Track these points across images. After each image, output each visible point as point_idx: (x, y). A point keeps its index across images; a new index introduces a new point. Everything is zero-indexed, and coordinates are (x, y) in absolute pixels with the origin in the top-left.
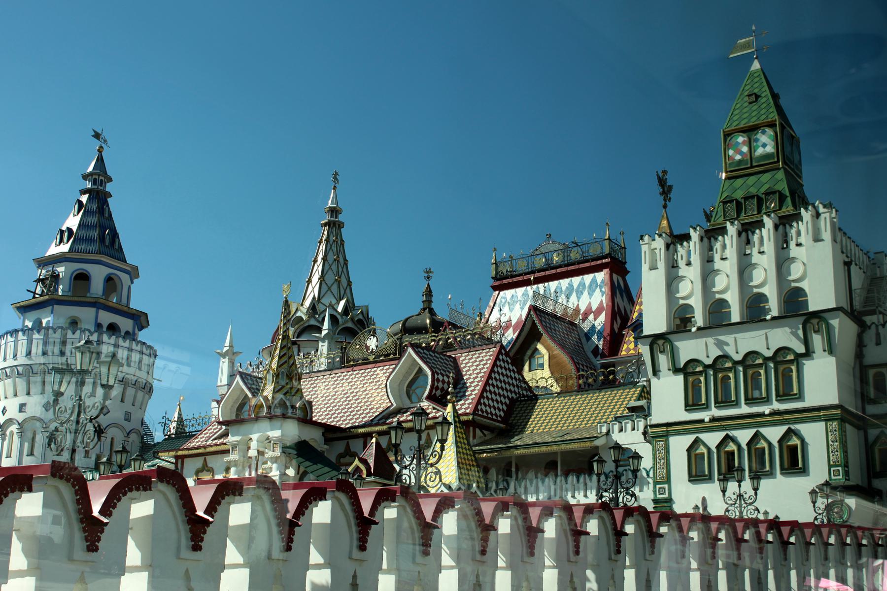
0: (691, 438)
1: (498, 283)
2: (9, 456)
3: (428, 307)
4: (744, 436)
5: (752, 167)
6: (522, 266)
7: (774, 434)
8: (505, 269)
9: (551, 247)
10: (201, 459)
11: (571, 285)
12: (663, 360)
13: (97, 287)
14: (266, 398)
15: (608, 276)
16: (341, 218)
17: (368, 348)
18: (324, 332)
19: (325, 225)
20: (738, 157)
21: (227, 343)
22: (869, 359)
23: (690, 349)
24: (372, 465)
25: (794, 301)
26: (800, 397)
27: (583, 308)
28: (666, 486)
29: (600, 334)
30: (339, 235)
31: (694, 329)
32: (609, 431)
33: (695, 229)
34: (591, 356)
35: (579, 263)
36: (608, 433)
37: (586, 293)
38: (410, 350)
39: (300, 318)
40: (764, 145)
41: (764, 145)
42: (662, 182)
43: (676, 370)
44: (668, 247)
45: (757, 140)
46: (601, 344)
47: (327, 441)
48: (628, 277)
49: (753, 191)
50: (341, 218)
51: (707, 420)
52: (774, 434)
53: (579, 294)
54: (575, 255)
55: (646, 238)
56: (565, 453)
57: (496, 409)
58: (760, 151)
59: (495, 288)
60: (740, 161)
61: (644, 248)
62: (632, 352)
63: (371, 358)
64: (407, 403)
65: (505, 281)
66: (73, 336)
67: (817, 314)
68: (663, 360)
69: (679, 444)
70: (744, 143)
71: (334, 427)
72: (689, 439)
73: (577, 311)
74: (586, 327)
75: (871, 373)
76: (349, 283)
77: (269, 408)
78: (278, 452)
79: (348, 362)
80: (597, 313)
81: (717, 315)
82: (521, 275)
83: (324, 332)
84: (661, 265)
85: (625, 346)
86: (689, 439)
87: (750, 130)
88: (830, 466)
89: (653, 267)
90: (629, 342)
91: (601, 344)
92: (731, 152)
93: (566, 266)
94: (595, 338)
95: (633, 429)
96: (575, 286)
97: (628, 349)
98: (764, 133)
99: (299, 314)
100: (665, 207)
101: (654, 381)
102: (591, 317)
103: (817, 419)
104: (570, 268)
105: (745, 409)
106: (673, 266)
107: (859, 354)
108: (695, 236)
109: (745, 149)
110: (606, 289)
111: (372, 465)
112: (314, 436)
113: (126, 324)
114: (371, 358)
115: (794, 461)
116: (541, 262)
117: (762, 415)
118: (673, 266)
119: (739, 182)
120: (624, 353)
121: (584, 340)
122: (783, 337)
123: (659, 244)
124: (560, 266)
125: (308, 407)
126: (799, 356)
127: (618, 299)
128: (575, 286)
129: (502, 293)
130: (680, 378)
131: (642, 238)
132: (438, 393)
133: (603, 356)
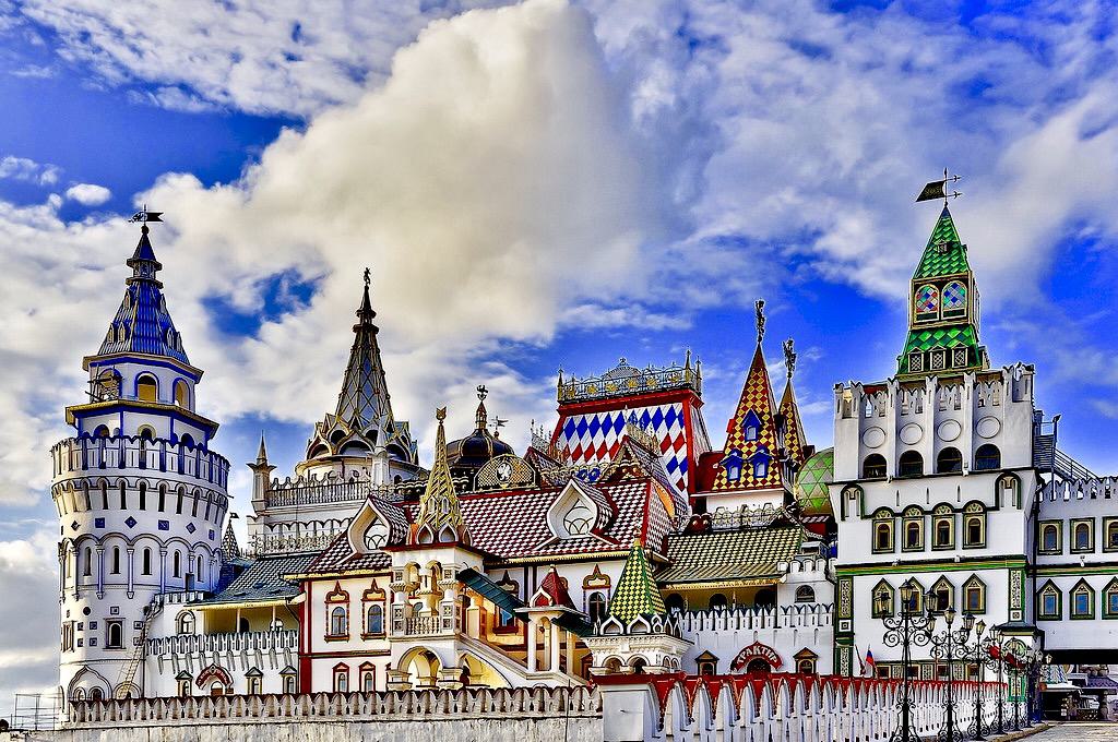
0: (876, 579)
2: (88, 573)
3: (481, 431)
10: (334, 582)
16: (374, 322)
17: (499, 476)
27: (661, 438)
28: (1012, 619)
36: (788, 571)
47: (486, 570)
62: (724, 487)
66: (153, 448)
67: (1008, 472)
69: (864, 586)
72: (874, 580)
78: (452, 579)
79: (477, 488)
85: (717, 482)
86: (874, 580)
90: (721, 478)
95: (814, 568)
97: (720, 485)
112: (476, 563)
113: (197, 436)
120: (715, 488)
122: (982, 488)
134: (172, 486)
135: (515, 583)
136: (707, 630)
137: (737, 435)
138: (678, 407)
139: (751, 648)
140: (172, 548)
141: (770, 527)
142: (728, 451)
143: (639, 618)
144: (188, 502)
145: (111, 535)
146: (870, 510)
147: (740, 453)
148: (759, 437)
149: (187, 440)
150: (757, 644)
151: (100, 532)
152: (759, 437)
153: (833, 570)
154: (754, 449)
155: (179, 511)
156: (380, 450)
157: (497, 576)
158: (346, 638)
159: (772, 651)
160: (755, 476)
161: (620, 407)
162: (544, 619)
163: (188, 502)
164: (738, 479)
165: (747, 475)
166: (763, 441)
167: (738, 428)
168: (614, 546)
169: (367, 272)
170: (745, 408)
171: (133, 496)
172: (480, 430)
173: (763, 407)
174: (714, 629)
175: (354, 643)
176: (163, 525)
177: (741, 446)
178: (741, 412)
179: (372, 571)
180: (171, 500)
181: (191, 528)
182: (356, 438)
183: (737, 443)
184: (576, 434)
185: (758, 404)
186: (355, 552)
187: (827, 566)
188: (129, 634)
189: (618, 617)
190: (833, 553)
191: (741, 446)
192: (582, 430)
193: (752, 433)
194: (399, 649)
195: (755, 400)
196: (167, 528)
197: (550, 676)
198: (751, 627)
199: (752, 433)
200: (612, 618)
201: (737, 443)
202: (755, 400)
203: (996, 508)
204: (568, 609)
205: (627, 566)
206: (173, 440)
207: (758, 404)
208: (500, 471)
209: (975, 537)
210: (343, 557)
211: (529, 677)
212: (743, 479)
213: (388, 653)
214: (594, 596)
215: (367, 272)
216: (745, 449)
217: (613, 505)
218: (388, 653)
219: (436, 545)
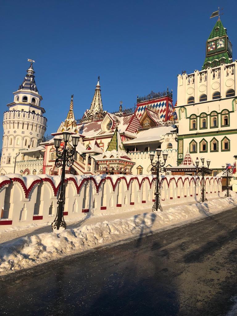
13: (29, 101)
20: (212, 49)
40: (221, 45)
41: (221, 45)
43: (187, 118)
48: (172, 102)
58: (219, 47)
68: (183, 115)
70: (214, 45)
80: (164, 112)
92: (209, 48)
98: (221, 40)
129: (139, 107)
134: (16, 122)
138: (165, 102)
140: (10, 138)
144: (30, 127)
145: (11, 135)
146: (188, 116)
149: (34, 112)
151: (15, 135)
155: (27, 129)
163: (30, 127)
169: (99, 77)
171: (16, 125)
176: (23, 132)
180: (25, 126)
181: (31, 134)
188: (12, 160)
190: (178, 132)
196: (24, 134)
205: (112, 139)
206: (30, 112)
209: (227, 123)
215: (99, 77)
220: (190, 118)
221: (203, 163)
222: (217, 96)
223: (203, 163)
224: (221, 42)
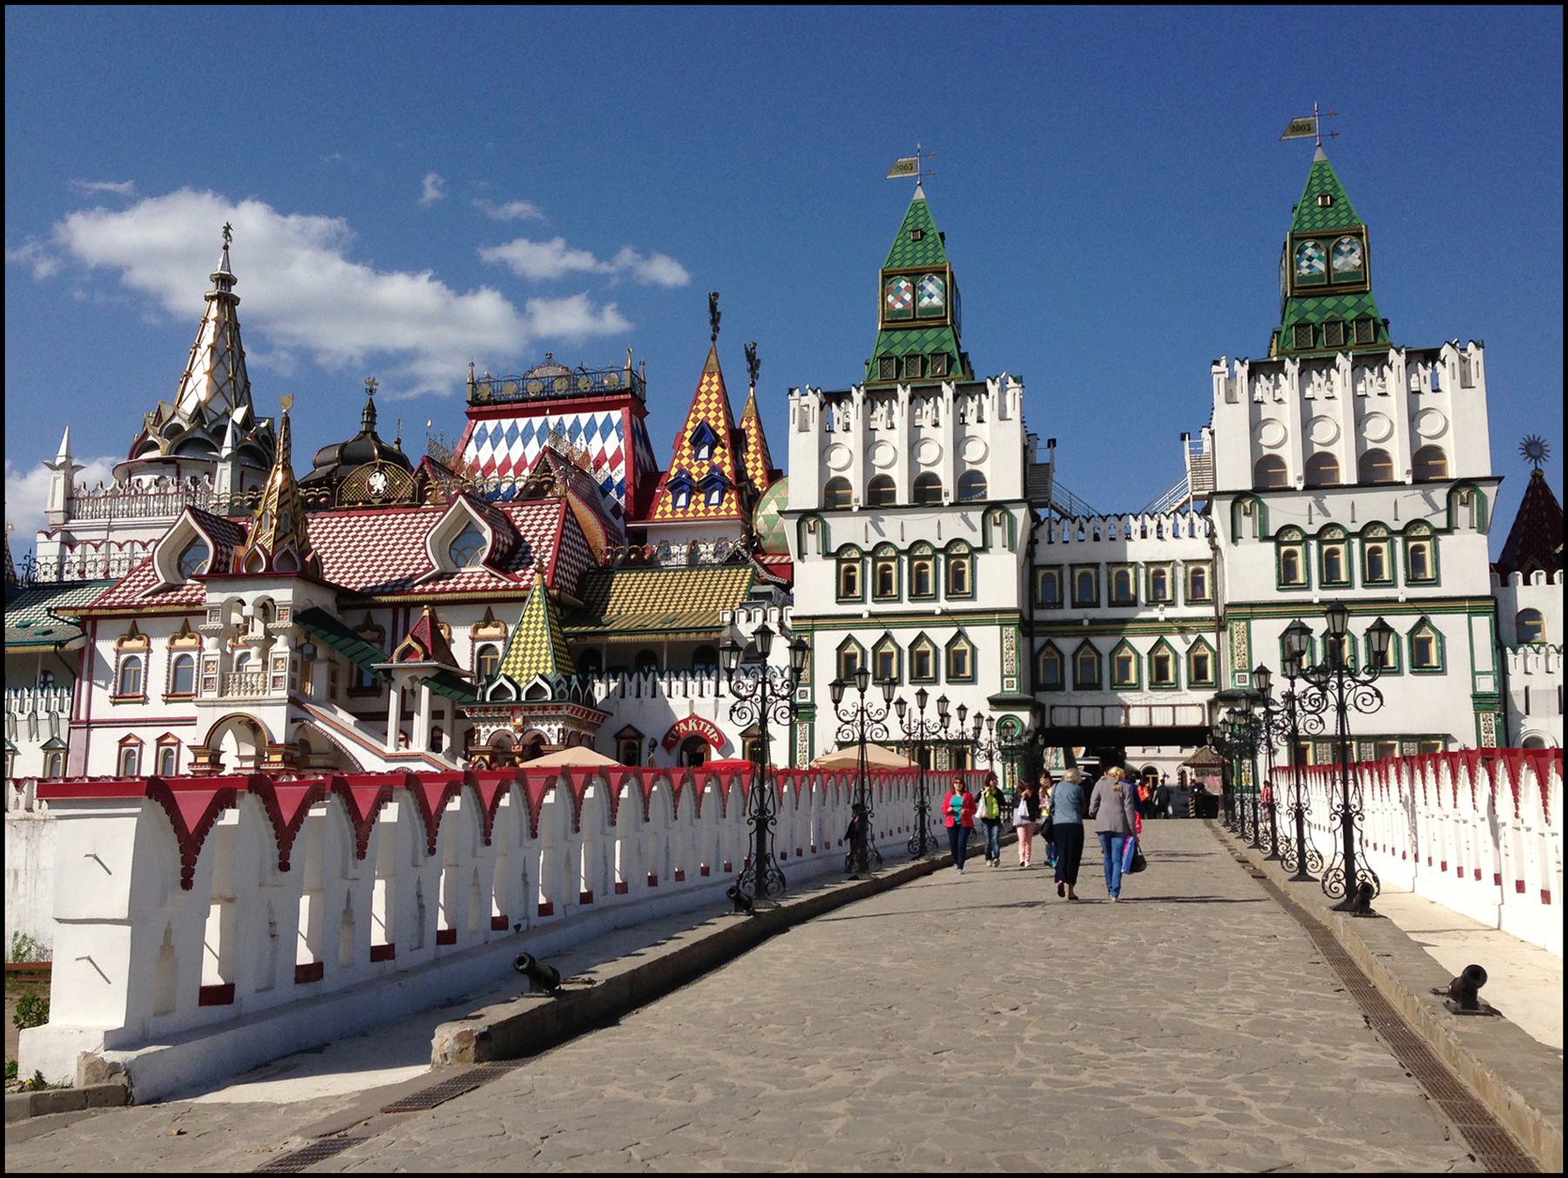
0: (841, 635)
1: (475, 409)
3: (370, 432)
4: (904, 637)
5: (915, 319)
6: (510, 390)
7: (941, 636)
8: (484, 392)
9: (551, 372)
11: (577, 422)
12: (812, 541)
14: (262, 547)
15: (627, 418)
16: (235, 290)
17: (371, 488)
18: (226, 452)
19: (212, 298)
20: (899, 306)
21: (63, 450)
22: (1038, 560)
23: (846, 529)
24: (428, 645)
25: (970, 485)
26: (972, 596)
27: (594, 453)
29: (620, 489)
30: (233, 313)
31: (855, 509)
32: (733, 619)
33: (858, 389)
34: (612, 517)
35: (589, 395)
37: (598, 435)
38: (461, 499)
39: (179, 428)
41: (931, 296)
42: (713, 307)
43: (827, 555)
44: (822, 407)
45: (922, 288)
46: (622, 501)
47: (341, 608)
49: (916, 348)
50: (235, 290)
51: (866, 615)
52: (941, 636)
53: (590, 431)
54: (583, 384)
55: (797, 392)
56: (671, 643)
57: (568, 579)
58: (925, 301)
59: (471, 415)
60: (900, 312)
61: (793, 404)
62: (669, 516)
63: (376, 502)
64: (451, 567)
65: (485, 408)
68: (812, 541)
71: (351, 591)
72: (839, 636)
73: (586, 454)
74: (600, 478)
75: (1041, 573)
76: (247, 385)
77: (269, 560)
78: (287, 622)
81: (879, 495)
82: (508, 402)
83: (226, 452)
84: (814, 427)
85: (660, 508)
86: (839, 636)
87: (914, 275)
88: (1003, 677)
89: (803, 429)
90: (665, 504)
91: (622, 501)
92: (890, 298)
93: (571, 397)
94: (613, 493)
96: (583, 425)
98: (931, 280)
99: (176, 420)
100: (714, 339)
101: (798, 565)
102: (606, 466)
103: (991, 623)
104: (577, 401)
105: (906, 606)
106: (826, 431)
107: (1030, 553)
108: (858, 396)
109: (908, 297)
110: (626, 432)
111: (428, 645)
112: (325, 601)
114: (376, 502)
115: (960, 668)
116: (534, 389)
117: (932, 614)
118: (826, 431)
119: (898, 336)
121: (599, 494)
123: (813, 400)
124: (563, 397)
125: (317, 562)
126: (974, 551)
127: (638, 448)
128: (583, 425)
129: (480, 423)
130: (832, 563)
131: (791, 392)
132: (498, 557)
133: (628, 519)
135: (381, 630)
136: (630, 698)
137: (686, 452)
138: (616, 416)
139: (686, 722)
141: (724, 565)
142: (674, 471)
143: (538, 680)
147: (689, 477)
148: (711, 454)
150: (693, 716)
152: (711, 454)
153: (789, 624)
154: (705, 470)
156: (229, 451)
157: (354, 619)
158: (145, 700)
159: (713, 726)
160: (707, 503)
161: (539, 412)
162: (413, 679)
164: (687, 506)
165: (697, 502)
166: (717, 460)
167: (686, 443)
168: (512, 584)
170: (695, 420)
172: (365, 433)
173: (717, 419)
174: (638, 696)
175: (156, 707)
177: (690, 466)
178: (690, 425)
179: (184, 608)
182: (199, 434)
183: (685, 461)
184: (503, 442)
185: (712, 414)
186: (163, 581)
187: (781, 618)
189: (509, 679)
190: (789, 601)
191: (690, 466)
192: (496, 438)
193: (704, 453)
194: (208, 718)
195: (707, 411)
197: (416, 758)
198: (685, 695)
199: (704, 453)
200: (503, 680)
201: (685, 461)
202: (707, 411)
203: (1449, 530)
204: (444, 666)
207: (712, 414)
208: (372, 481)
210: (146, 587)
211: (389, 758)
212: (692, 507)
213: (190, 721)
214: (483, 650)
215: (227, 228)
216: (694, 470)
217: (515, 531)
218: (190, 721)
219: (273, 575)
220: (838, 555)
221: (962, 720)
222: (925, 493)
223: (962, 720)
224: (930, 288)
